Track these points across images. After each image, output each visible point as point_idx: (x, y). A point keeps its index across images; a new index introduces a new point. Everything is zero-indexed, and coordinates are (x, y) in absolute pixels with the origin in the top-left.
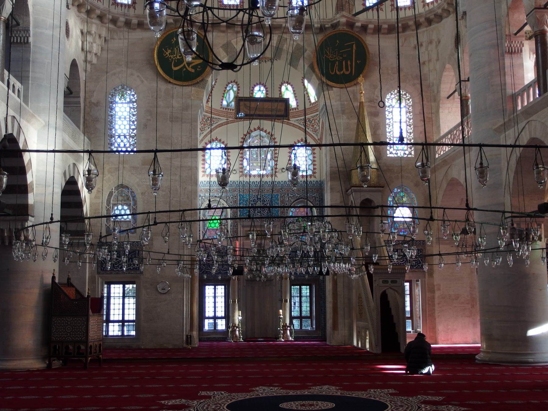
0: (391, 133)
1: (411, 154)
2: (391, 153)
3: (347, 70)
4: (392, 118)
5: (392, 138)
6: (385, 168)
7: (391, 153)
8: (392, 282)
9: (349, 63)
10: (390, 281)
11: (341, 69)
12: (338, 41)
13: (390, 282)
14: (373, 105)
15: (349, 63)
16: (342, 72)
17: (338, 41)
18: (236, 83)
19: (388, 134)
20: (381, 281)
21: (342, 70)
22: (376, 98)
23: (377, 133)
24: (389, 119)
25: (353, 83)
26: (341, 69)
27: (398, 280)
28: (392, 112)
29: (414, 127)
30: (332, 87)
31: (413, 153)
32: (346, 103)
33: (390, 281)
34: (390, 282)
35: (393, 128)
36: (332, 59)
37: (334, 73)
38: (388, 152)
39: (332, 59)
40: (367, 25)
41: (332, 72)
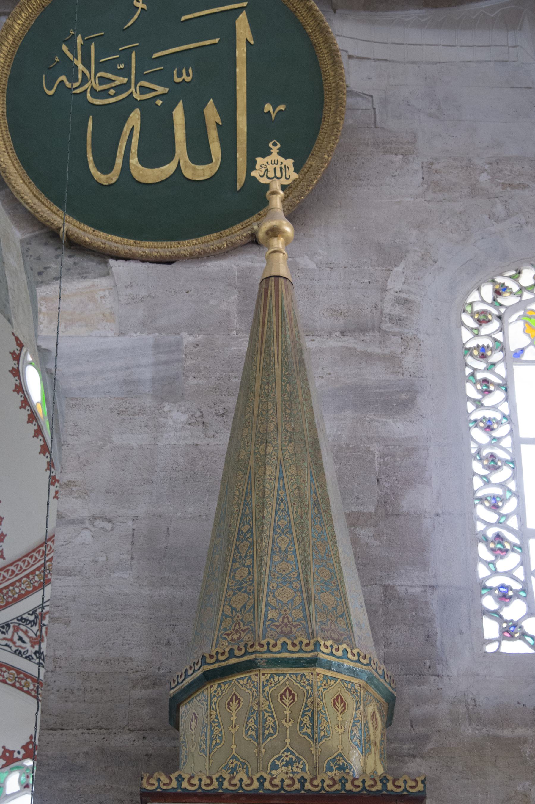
2: (511, 631)
3: (199, 153)
4: (510, 419)
6: (468, 731)
7: (511, 631)
9: (212, 114)
11: (156, 150)
12: (140, 5)
14: (374, 349)
15: (212, 114)
16: (169, 169)
19: (482, 512)
21: (169, 154)
22: (398, 311)
23: (408, 502)
24: (489, 427)
25: (238, 233)
26: (156, 150)
28: (506, 387)
30: (104, 255)
32: (187, 339)
35: (517, 474)
36: (104, 94)
37: (113, 177)
38: (490, 628)
41: (106, 166)
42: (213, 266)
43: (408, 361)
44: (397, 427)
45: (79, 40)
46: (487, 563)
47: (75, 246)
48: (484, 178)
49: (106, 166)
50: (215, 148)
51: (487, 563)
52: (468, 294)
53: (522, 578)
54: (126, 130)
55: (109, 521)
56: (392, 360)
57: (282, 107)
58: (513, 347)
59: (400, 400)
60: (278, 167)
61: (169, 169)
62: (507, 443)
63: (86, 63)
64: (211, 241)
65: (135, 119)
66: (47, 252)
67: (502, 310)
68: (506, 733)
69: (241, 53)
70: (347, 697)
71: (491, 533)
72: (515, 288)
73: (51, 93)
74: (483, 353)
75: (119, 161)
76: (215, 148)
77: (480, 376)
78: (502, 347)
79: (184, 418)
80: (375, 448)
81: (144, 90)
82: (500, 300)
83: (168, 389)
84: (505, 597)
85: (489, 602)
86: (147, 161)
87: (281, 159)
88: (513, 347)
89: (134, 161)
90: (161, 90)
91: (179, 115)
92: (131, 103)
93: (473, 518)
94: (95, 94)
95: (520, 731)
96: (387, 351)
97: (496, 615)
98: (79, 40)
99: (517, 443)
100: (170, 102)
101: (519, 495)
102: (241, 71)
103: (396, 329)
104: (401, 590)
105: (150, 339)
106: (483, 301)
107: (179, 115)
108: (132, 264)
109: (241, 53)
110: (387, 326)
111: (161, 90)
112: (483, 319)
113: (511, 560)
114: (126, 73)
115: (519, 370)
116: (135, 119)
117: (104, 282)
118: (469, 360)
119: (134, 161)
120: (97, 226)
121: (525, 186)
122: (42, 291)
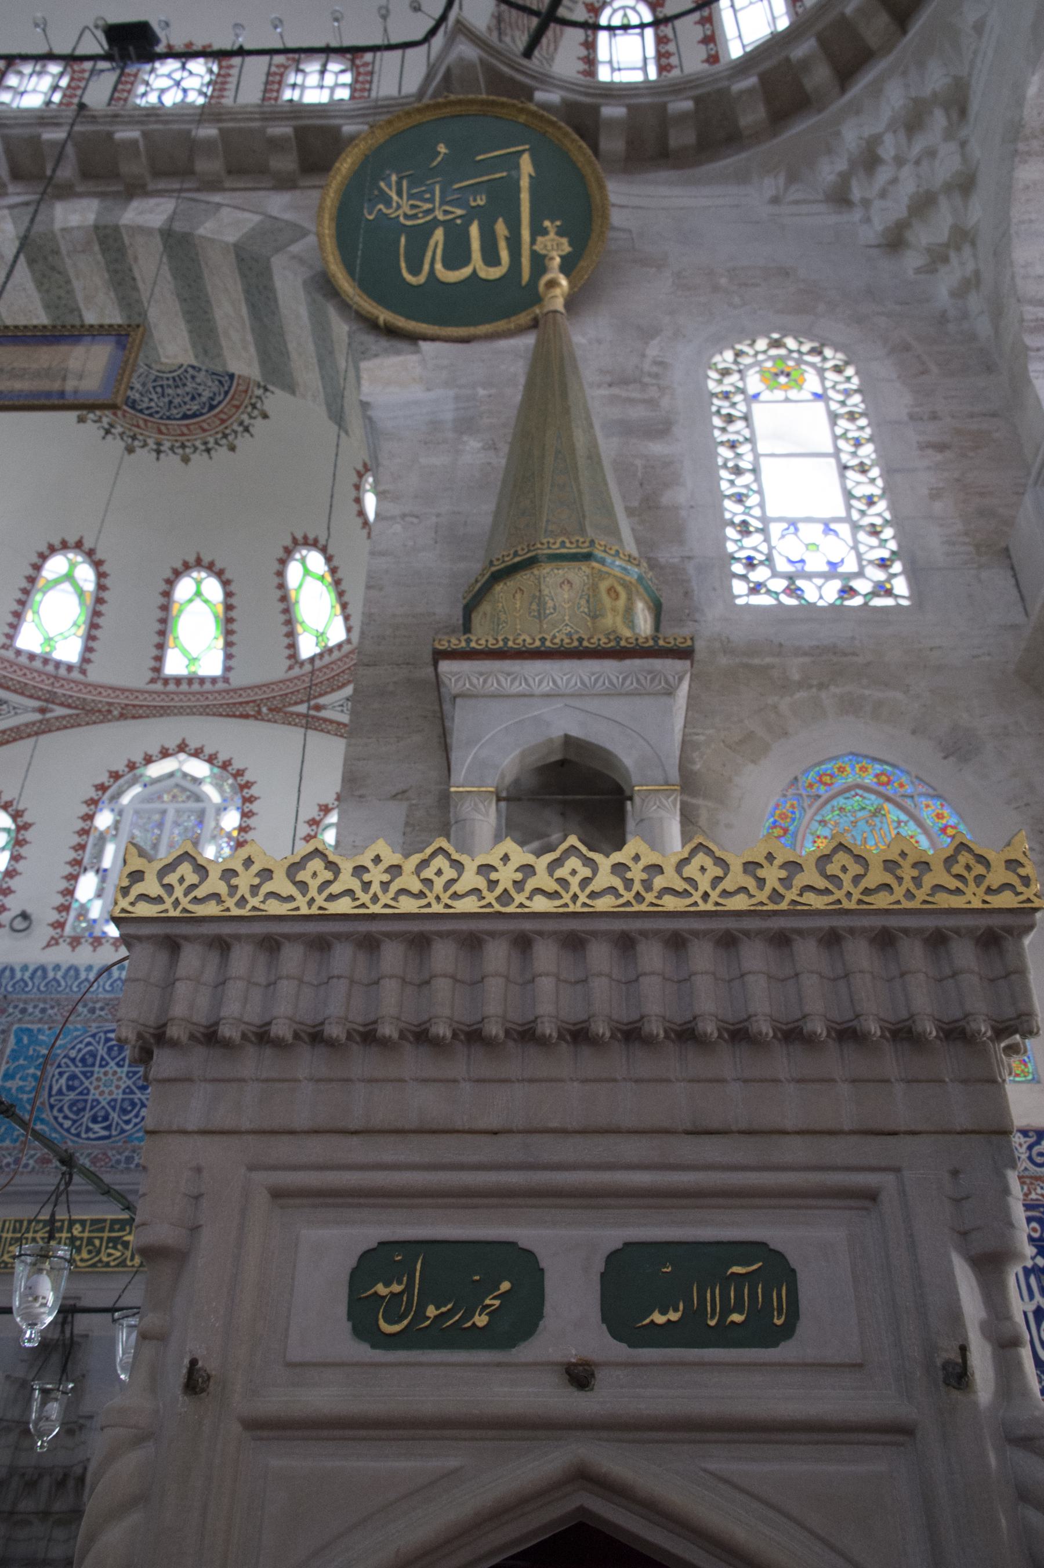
0: (753, 500)
1: (889, 593)
3: (491, 257)
4: (751, 440)
5: (755, 524)
6: (724, 661)
8: (631, 1287)
9: (501, 229)
10: (572, 1258)
12: (442, 149)
13: (572, 1315)
14: (636, 395)
15: (501, 229)
16: (466, 272)
17: (442, 149)
18: (90, 554)
20: (332, 1246)
21: (466, 260)
22: (655, 369)
23: (666, 499)
24: (733, 445)
25: (524, 318)
27: (815, 1246)
28: (746, 418)
29: (888, 473)
30: (413, 338)
31: (900, 586)
32: (481, 392)
33: (572, 1258)
34: (572, 1315)
35: (757, 480)
36: (414, 217)
37: (422, 279)
38: (739, 587)
39: (414, 217)
40: (595, 109)
41: (415, 270)
42: (503, 344)
43: (665, 402)
44: (657, 448)
45: (394, 178)
46: (736, 541)
47: (391, 332)
48: (723, 281)
49: (415, 270)
50: (504, 255)
51: (736, 541)
52: (712, 356)
53: (766, 551)
54: (432, 242)
55: (417, 517)
56: (652, 403)
57: (558, 223)
58: (751, 391)
59: (661, 429)
60: (555, 244)
61: (466, 272)
62: (749, 457)
63: (399, 194)
64: (501, 325)
65: (439, 235)
66: (369, 340)
67: (742, 367)
68: (756, 661)
69: (525, 183)
70: (619, 589)
71: (737, 520)
72: (751, 352)
73: (371, 217)
74: (726, 396)
75: (426, 267)
76: (504, 255)
77: (724, 411)
78: (743, 391)
79: (479, 445)
80: (639, 462)
81: (446, 212)
82: (740, 360)
83: (465, 425)
84: (750, 563)
85: (738, 568)
86: (450, 264)
87: (556, 238)
88: (751, 391)
89: (439, 266)
90: (459, 212)
91: (474, 230)
92: (435, 223)
93: (722, 509)
94: (406, 216)
95: (768, 660)
96: (646, 396)
97: (744, 577)
98: (394, 178)
99: (757, 456)
100: (467, 221)
101: (760, 492)
102: (525, 197)
103: (654, 381)
104: (662, 561)
105: (451, 393)
106: (724, 361)
107: (474, 230)
108: (438, 345)
109: (525, 183)
110: (646, 380)
111: (459, 212)
112: (725, 373)
113: (756, 539)
114: (431, 200)
115: (756, 407)
116: (439, 235)
117: (415, 358)
118: (715, 401)
119: (439, 266)
120: (409, 317)
121: (757, 285)
122: (364, 365)
